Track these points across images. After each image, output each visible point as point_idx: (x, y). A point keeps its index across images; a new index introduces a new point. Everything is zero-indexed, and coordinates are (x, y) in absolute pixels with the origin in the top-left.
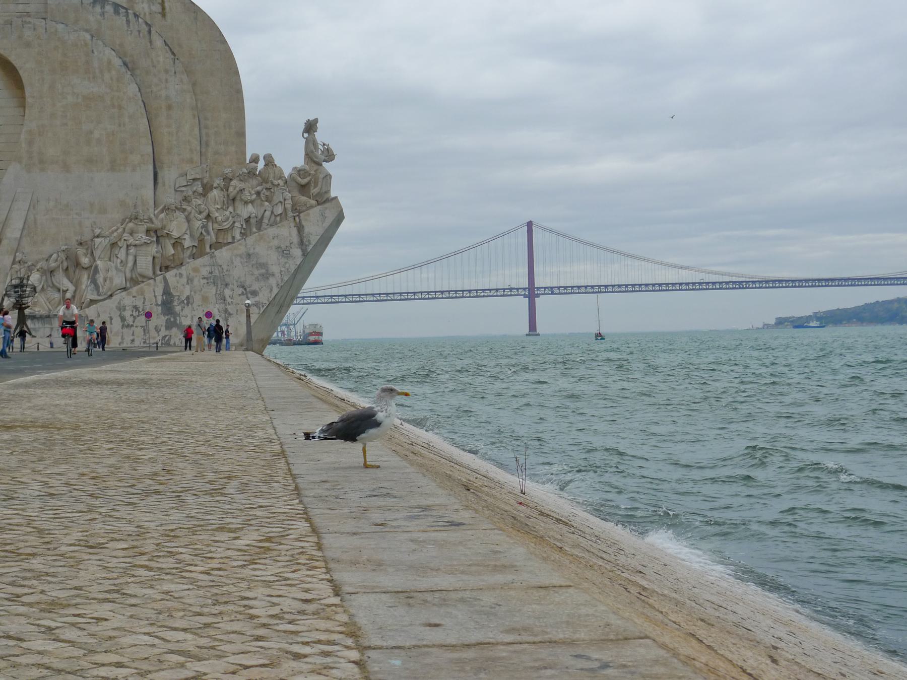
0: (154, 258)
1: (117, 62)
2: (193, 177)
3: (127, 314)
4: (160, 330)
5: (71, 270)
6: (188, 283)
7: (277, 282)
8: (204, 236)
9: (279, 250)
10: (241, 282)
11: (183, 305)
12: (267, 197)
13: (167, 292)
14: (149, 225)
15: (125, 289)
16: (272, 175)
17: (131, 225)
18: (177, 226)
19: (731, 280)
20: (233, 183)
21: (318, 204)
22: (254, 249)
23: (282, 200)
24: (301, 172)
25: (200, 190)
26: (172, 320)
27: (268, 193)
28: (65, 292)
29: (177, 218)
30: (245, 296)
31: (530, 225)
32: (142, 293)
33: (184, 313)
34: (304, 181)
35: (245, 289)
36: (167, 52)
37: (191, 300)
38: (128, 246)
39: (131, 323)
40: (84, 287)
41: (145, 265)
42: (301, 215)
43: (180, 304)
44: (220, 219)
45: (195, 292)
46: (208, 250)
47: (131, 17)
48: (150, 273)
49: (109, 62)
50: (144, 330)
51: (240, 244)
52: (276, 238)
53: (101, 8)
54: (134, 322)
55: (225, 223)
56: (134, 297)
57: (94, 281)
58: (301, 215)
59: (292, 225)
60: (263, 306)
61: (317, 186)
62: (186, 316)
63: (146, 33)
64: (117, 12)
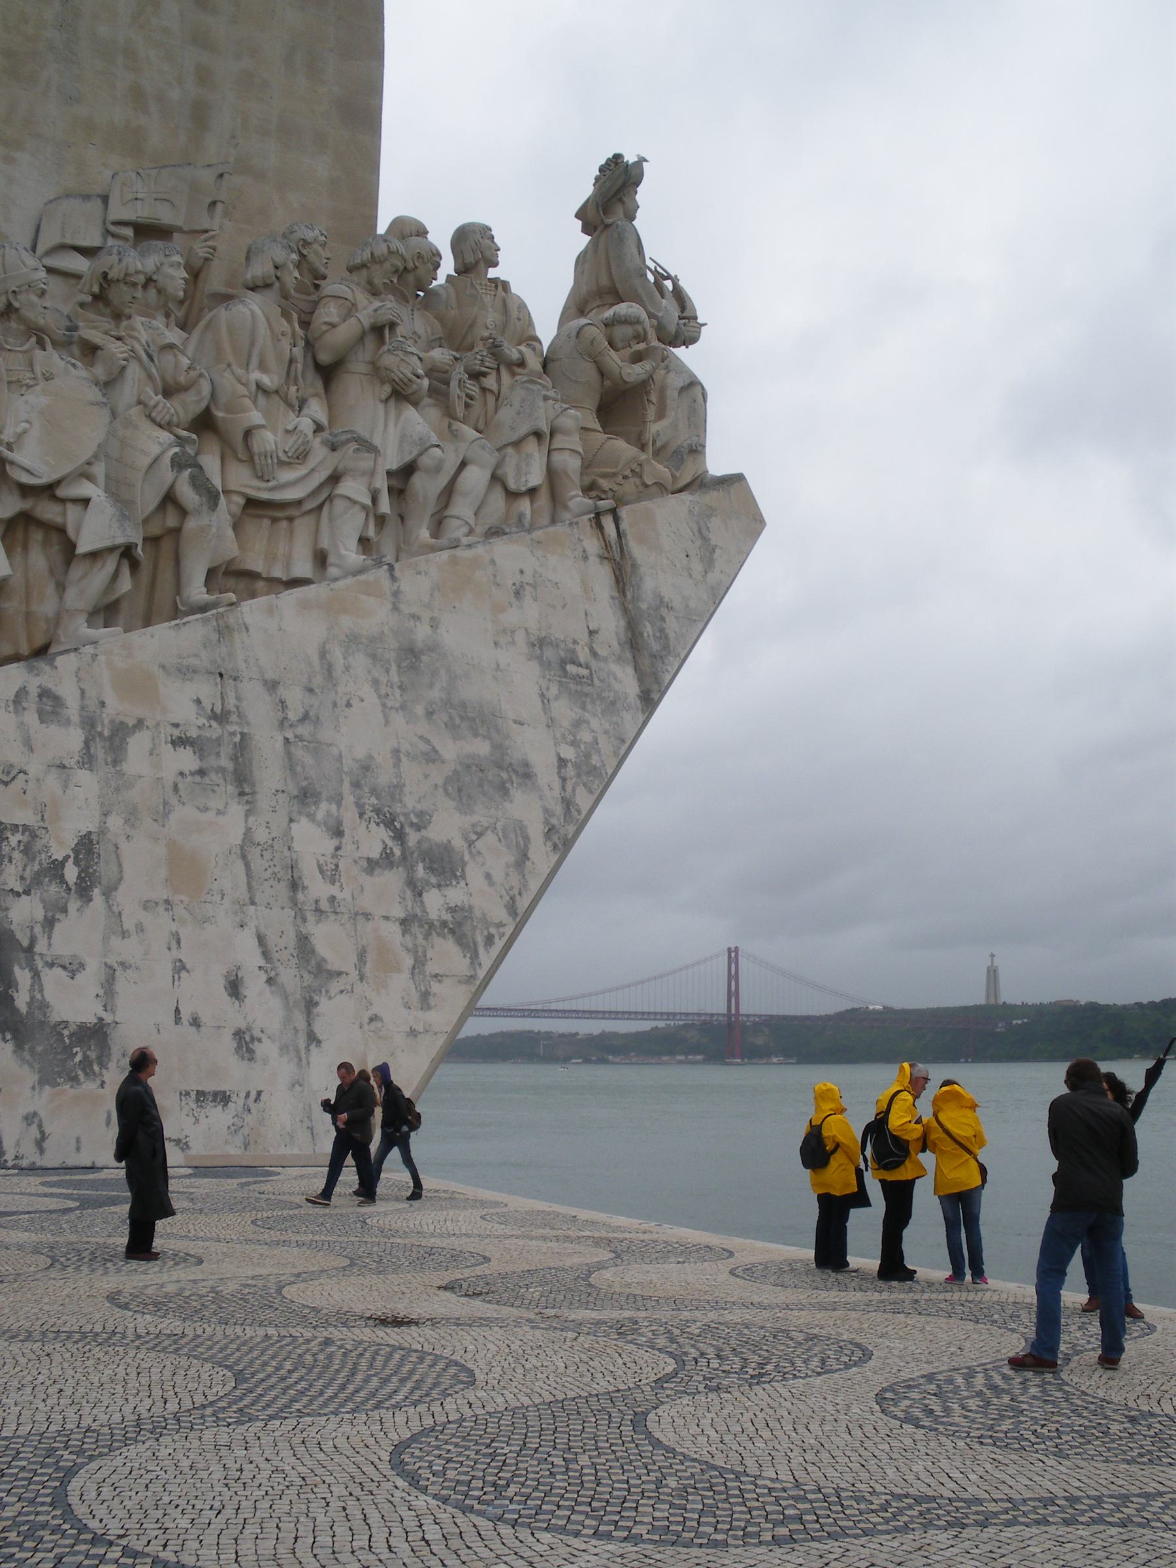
6: (87, 760)
7: (546, 811)
8: (183, 512)
9: (549, 653)
10: (374, 792)
11: (54, 889)
16: (492, 317)
22: (434, 624)
23: (546, 429)
29: (48, 378)
34: (635, 372)
37: (105, 869)
43: (37, 879)
44: (267, 440)
45: (132, 817)
55: (286, 475)
58: (624, 512)
59: (592, 545)
60: (489, 940)
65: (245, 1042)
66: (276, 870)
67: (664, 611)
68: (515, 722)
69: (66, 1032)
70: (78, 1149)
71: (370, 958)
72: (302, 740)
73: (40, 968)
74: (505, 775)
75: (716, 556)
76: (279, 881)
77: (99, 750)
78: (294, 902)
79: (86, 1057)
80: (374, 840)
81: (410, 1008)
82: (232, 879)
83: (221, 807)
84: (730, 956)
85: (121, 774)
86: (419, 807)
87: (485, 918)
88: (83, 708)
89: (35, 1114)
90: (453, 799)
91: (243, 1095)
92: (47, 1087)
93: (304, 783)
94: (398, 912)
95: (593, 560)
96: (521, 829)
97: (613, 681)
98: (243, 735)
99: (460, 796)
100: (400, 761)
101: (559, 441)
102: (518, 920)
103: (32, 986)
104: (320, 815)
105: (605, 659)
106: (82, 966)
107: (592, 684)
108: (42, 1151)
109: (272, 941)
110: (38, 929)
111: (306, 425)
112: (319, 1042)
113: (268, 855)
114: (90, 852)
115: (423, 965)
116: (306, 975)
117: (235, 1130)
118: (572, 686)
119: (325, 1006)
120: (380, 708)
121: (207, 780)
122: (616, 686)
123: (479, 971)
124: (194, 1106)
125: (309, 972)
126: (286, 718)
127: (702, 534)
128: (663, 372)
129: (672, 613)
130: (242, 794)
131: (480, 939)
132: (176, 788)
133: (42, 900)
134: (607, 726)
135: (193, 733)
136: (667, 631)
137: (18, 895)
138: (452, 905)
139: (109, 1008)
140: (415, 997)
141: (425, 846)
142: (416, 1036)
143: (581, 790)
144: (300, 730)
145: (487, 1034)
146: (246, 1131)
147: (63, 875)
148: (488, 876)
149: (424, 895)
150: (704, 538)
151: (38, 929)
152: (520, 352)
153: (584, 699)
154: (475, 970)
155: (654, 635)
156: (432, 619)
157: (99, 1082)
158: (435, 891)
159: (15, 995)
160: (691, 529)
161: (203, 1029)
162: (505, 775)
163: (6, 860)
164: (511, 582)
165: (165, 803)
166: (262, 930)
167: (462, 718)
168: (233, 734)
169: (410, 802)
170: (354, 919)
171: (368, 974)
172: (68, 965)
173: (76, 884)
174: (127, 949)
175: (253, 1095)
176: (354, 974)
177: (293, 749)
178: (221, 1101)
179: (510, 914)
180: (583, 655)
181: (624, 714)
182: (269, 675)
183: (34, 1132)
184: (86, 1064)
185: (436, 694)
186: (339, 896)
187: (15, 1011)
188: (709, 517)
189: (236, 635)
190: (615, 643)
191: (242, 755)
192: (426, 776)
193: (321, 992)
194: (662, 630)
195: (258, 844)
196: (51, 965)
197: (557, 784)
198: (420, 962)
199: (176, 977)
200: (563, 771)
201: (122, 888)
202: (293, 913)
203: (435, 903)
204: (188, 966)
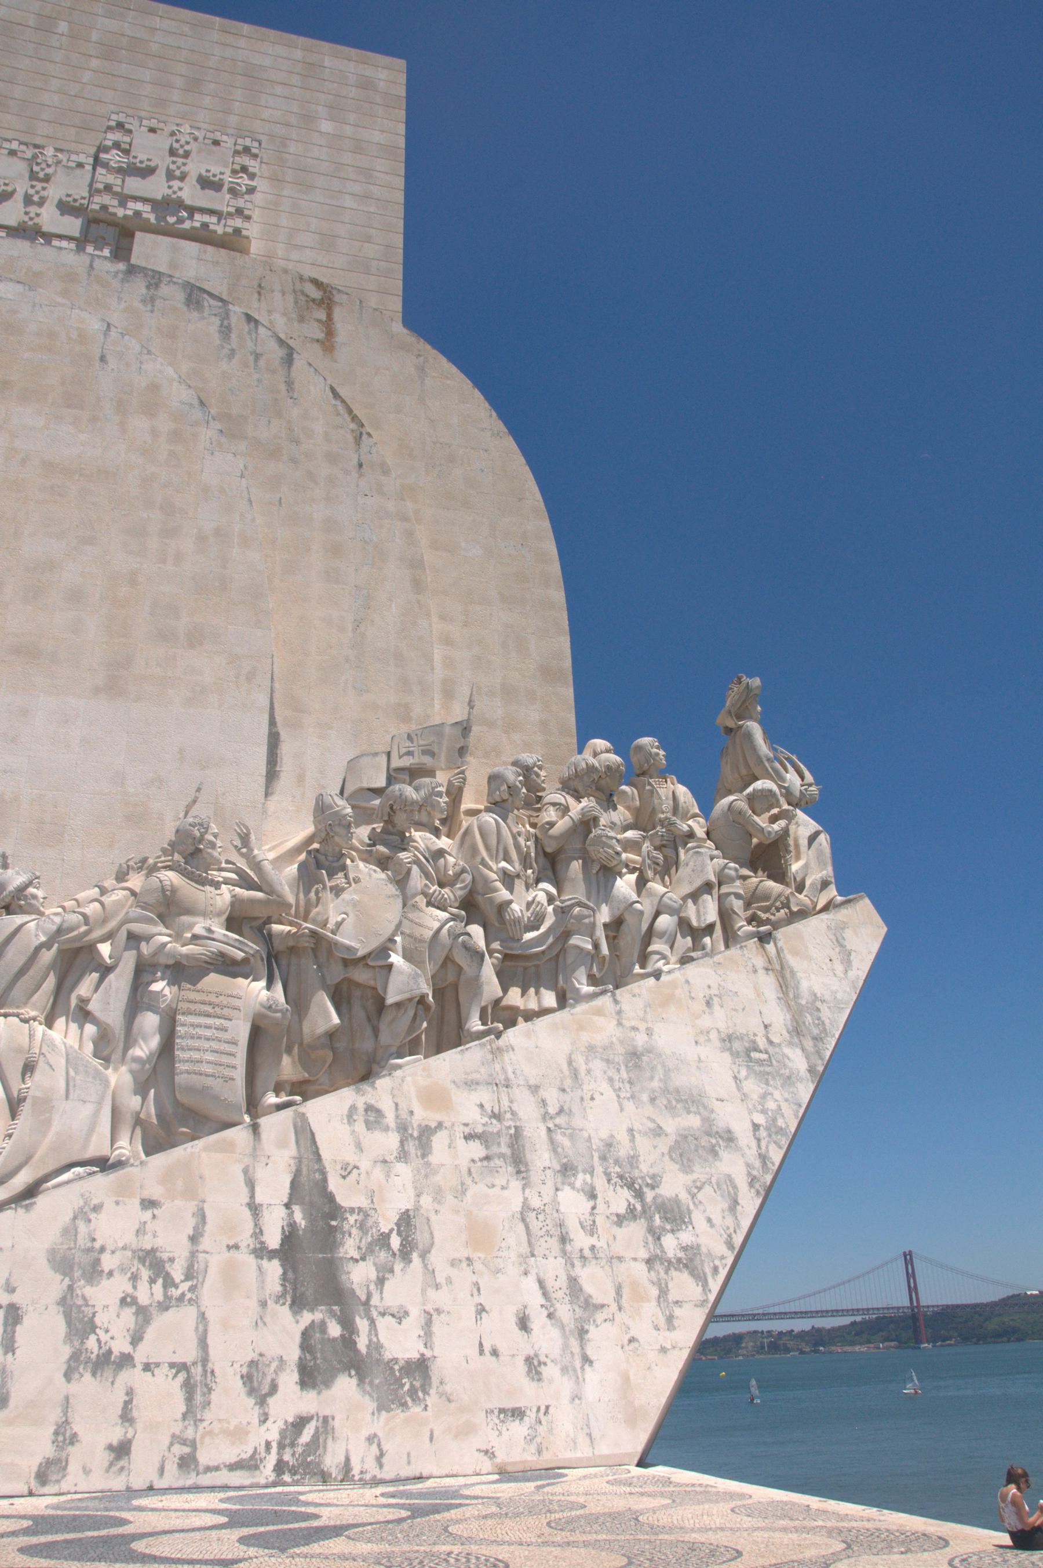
1: (179, 395)
4: (274, 1388)
6: (403, 1156)
7: (748, 1165)
9: (737, 1045)
10: (617, 1162)
11: (383, 1255)
22: (649, 1032)
26: (335, 1330)
30: (643, 1222)
36: (338, 414)
37: (420, 1237)
39: (120, 1346)
42: (780, 934)
45: (438, 1195)
49: (154, 388)
50: (189, 1388)
51: (599, 1012)
52: (716, 1000)
53: (148, 288)
54: (136, 1339)
56: (149, 1204)
59: (760, 962)
60: (715, 1270)
62: (400, 1316)
65: (533, 1366)
66: (549, 1228)
67: (819, 1004)
68: (717, 1100)
69: (396, 1367)
70: (409, 1463)
71: (626, 1292)
72: (560, 1128)
73: (375, 1317)
74: (714, 1141)
75: (852, 958)
76: (551, 1236)
77: (411, 1147)
78: (564, 1252)
79: (412, 1385)
80: (620, 1200)
81: (659, 1330)
82: (514, 1239)
83: (504, 1183)
85: (428, 1164)
86: (652, 1171)
87: (710, 1254)
88: (397, 1117)
89: (375, 1435)
90: (677, 1163)
91: (534, 1410)
92: (384, 1413)
93: (565, 1160)
94: (644, 1254)
95: (761, 972)
96: (730, 1181)
97: (787, 1061)
98: (516, 1128)
99: (682, 1160)
100: (633, 1136)
101: (725, 889)
102: (735, 1253)
103: (370, 1331)
104: (578, 1184)
105: (779, 1045)
106: (406, 1313)
107: (771, 1065)
108: (381, 1466)
109: (550, 1283)
110: (372, 1287)
111: (542, 897)
112: (591, 1362)
113: (541, 1217)
114: (408, 1224)
115: (666, 1295)
116: (577, 1309)
117: (530, 1439)
118: (757, 1068)
119: (593, 1333)
120: (615, 1098)
121: (492, 1164)
122: (790, 1064)
123: (709, 1295)
124: (497, 1421)
125: (580, 1307)
126: (547, 1113)
127: (840, 943)
128: (794, 827)
129: (825, 1004)
130: (519, 1172)
131: (708, 1270)
132: (470, 1172)
133: (375, 1264)
134: (786, 1095)
135: (479, 1129)
136: (823, 1019)
137: (357, 1261)
138: (684, 1245)
139: (428, 1345)
140: (662, 1322)
141: (659, 1200)
142: (665, 1352)
143: (772, 1147)
144: (558, 1121)
146: (538, 1439)
147: (389, 1245)
148: (709, 1220)
149: (662, 1238)
150: (841, 946)
151: (372, 1287)
152: (689, 826)
153: (766, 1077)
154: (706, 1295)
155: (813, 1022)
156: (648, 1029)
157: (423, 1406)
158: (670, 1236)
159: (357, 1340)
160: (831, 940)
161: (501, 1358)
162: (714, 1141)
163: (347, 1235)
164: (702, 995)
165: (462, 1184)
166: (542, 1275)
167: (678, 1101)
168: (509, 1128)
169: (644, 1168)
170: (611, 1262)
171: (625, 1305)
172: (396, 1314)
173: (399, 1250)
174: (439, 1298)
175: (543, 1409)
176: (614, 1307)
177: (554, 1135)
178: (518, 1415)
179: (729, 1249)
180: (762, 1043)
181: (798, 1084)
182: (532, 1082)
183: (374, 1449)
184: (413, 1392)
185: (656, 1084)
186: (598, 1245)
187: (356, 1351)
188: (843, 929)
189: (505, 1054)
190: (785, 1033)
191: (517, 1143)
192: (655, 1147)
193: (589, 1321)
194: (819, 1019)
195: (534, 1210)
196: (383, 1314)
197: (754, 1144)
198: (663, 1292)
199: (478, 1317)
200: (757, 1133)
201: (433, 1251)
202: (563, 1261)
203: (670, 1244)
204: (487, 1308)
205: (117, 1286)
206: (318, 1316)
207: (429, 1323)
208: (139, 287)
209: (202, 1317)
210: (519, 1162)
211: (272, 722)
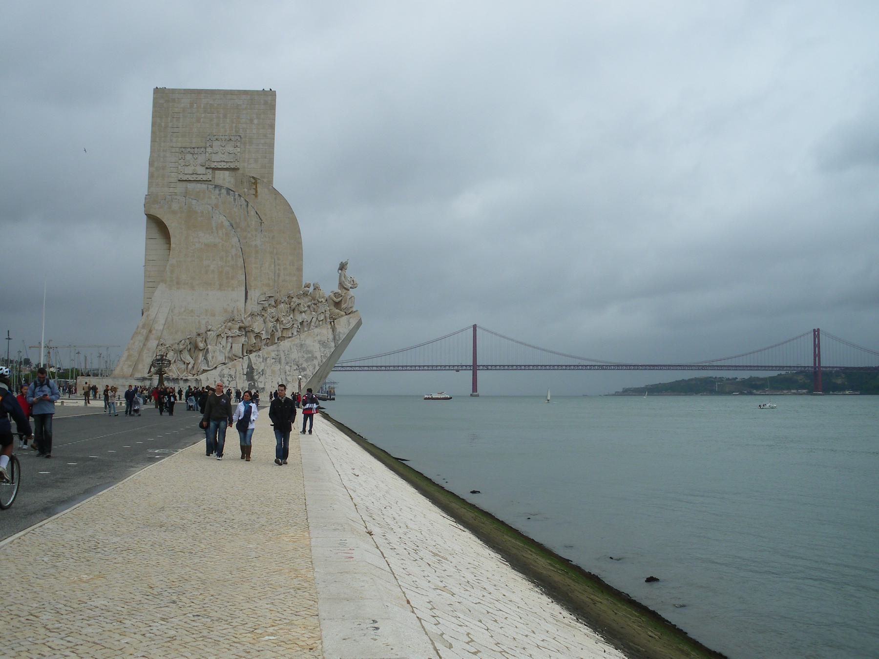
0: (243, 345)
1: (227, 224)
2: (269, 295)
3: (225, 380)
5: (193, 350)
6: (263, 362)
9: (321, 342)
12: (314, 309)
13: (250, 367)
14: (241, 324)
15: (224, 364)
17: (230, 324)
18: (258, 326)
19: (596, 364)
20: (293, 300)
21: (346, 315)
22: (305, 341)
23: (323, 311)
24: (336, 294)
25: (273, 303)
26: (253, 384)
27: (315, 307)
28: (188, 364)
31: (475, 327)
32: (234, 366)
33: (260, 380)
34: (337, 300)
35: (299, 367)
37: (265, 372)
38: (227, 337)
39: (227, 385)
40: (199, 361)
41: (237, 349)
44: (284, 322)
46: (276, 341)
47: (237, 196)
48: (241, 355)
51: (297, 338)
54: (229, 384)
55: (288, 325)
57: (206, 359)
59: (329, 326)
60: (309, 378)
61: (346, 303)
63: (245, 206)
64: (228, 194)
77: (264, 360)
84: (814, 334)
111: (289, 318)
145: (687, 379)
174: (267, 380)
185: (305, 350)
205: (227, 379)
206: (251, 382)
207: (265, 384)
208: (217, 191)
209: (236, 382)
210: (280, 362)
211: (246, 289)
